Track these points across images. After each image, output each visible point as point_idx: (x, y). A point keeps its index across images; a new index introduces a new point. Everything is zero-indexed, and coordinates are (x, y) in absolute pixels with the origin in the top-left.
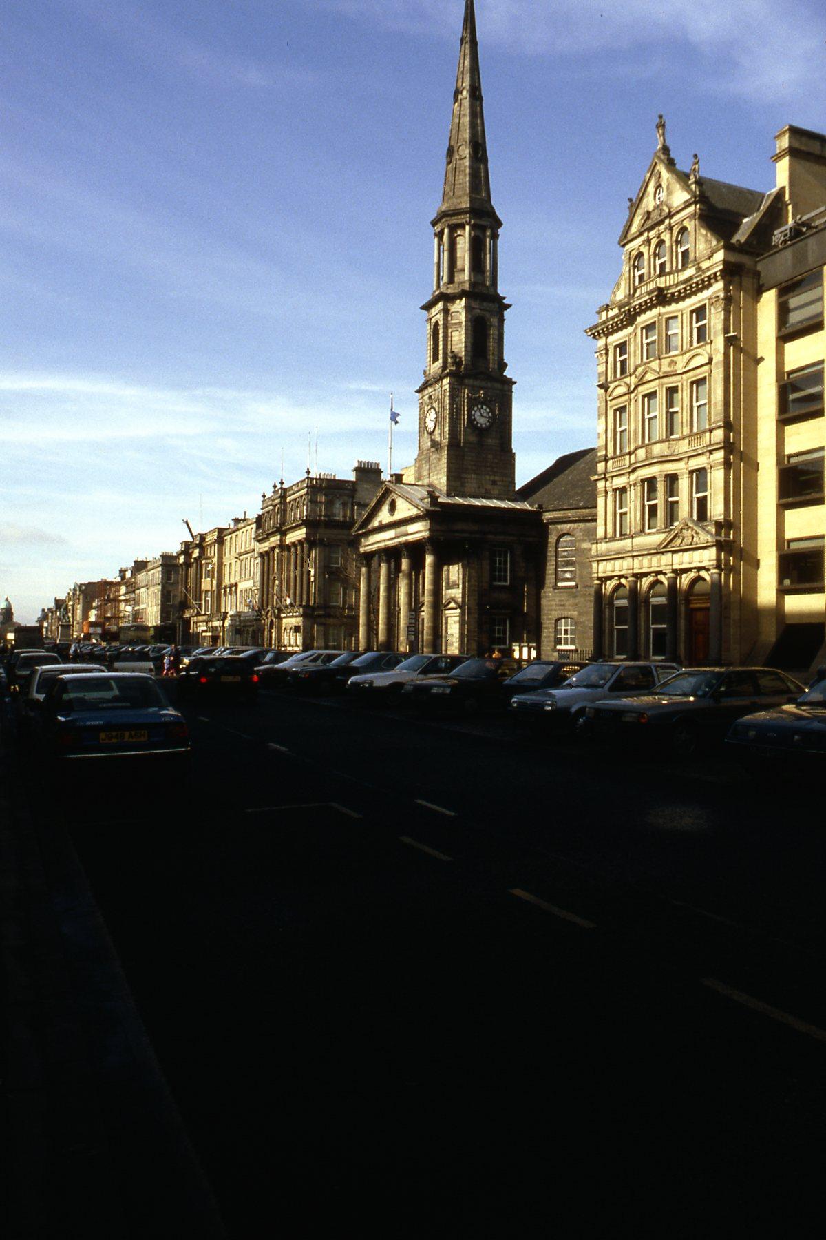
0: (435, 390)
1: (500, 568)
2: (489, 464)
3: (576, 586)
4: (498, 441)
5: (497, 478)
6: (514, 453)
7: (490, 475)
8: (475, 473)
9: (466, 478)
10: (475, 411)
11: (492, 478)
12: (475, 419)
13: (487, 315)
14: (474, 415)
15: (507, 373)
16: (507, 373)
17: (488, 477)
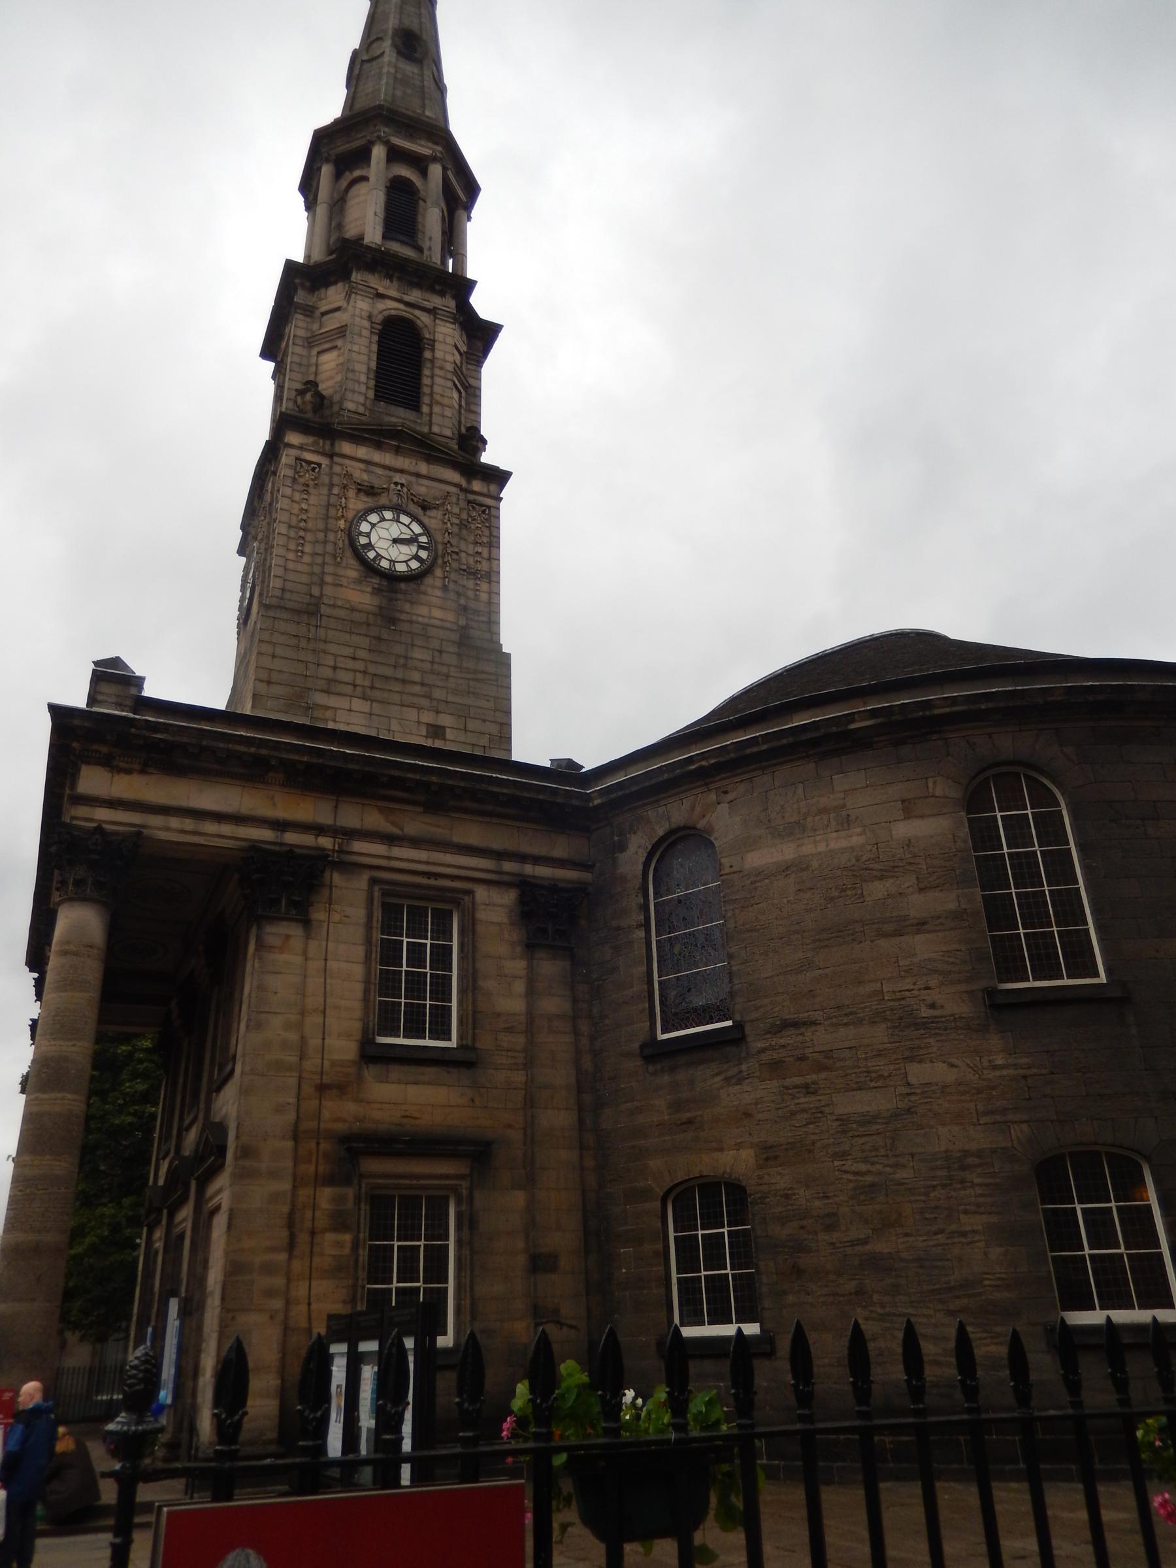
1: (416, 982)
2: (416, 676)
3: (739, 1027)
4: (451, 617)
5: (445, 720)
6: (508, 655)
7: (420, 709)
8: (364, 698)
9: (327, 708)
10: (373, 525)
11: (427, 717)
12: (369, 546)
13: (424, 318)
14: (368, 535)
15: (487, 458)
16: (487, 458)
17: (412, 714)
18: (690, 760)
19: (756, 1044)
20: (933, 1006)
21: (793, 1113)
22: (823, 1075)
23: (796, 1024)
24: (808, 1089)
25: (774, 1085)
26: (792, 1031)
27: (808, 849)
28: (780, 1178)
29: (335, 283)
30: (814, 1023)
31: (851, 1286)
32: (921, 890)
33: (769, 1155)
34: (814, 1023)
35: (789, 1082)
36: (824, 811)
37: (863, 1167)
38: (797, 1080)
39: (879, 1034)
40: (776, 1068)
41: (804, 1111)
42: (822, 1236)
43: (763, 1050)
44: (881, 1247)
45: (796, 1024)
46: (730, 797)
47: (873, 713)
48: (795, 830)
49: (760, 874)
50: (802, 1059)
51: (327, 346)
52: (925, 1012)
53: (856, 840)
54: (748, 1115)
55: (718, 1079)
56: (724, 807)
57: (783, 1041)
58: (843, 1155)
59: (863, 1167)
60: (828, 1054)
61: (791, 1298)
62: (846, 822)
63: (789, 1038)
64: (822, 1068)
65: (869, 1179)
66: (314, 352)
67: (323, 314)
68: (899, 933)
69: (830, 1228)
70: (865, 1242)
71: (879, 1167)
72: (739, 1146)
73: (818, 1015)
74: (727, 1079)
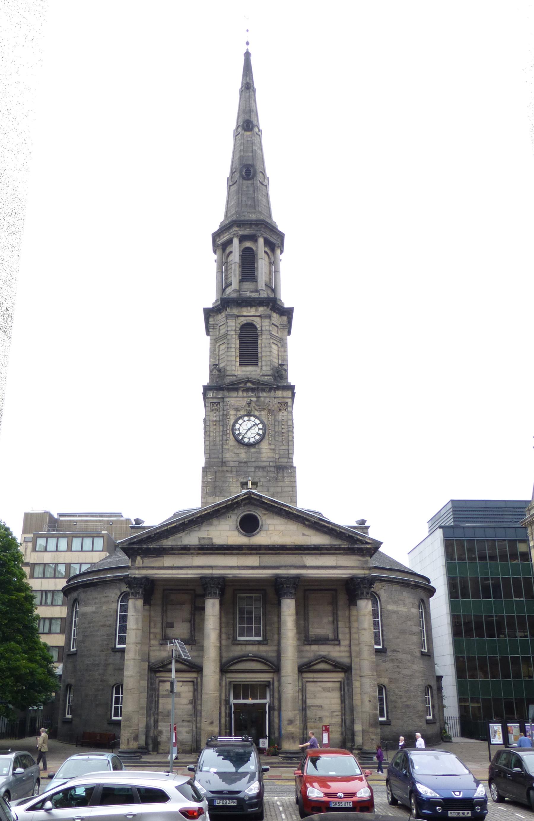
0: (258, 397)
18: (383, 577)
19: (389, 654)
20: (416, 653)
21: (395, 672)
22: (401, 664)
23: (396, 651)
24: (398, 667)
25: (392, 664)
26: (395, 653)
27: (399, 609)
28: (393, 686)
29: (277, 313)
30: (399, 652)
31: (404, 711)
32: (415, 625)
33: (391, 681)
34: (399, 652)
35: (394, 664)
36: (401, 600)
37: (406, 686)
38: (396, 664)
39: (408, 657)
40: (392, 660)
41: (397, 672)
42: (400, 700)
43: (390, 656)
44: (408, 703)
45: (396, 651)
46: (384, 588)
47: (415, 582)
48: (396, 603)
49: (390, 612)
50: (397, 659)
51: (275, 342)
52: (415, 654)
53: (406, 610)
54: (387, 670)
55: (381, 660)
56: (382, 590)
57: (394, 655)
58: (403, 683)
59: (406, 686)
60: (401, 659)
61: (394, 713)
62: (405, 605)
63: (394, 654)
64: (401, 663)
65: (407, 688)
66: (272, 341)
67: (273, 324)
68: (411, 634)
69: (401, 698)
70: (406, 702)
71: (408, 686)
72: (385, 677)
73: (400, 650)
74: (383, 661)
